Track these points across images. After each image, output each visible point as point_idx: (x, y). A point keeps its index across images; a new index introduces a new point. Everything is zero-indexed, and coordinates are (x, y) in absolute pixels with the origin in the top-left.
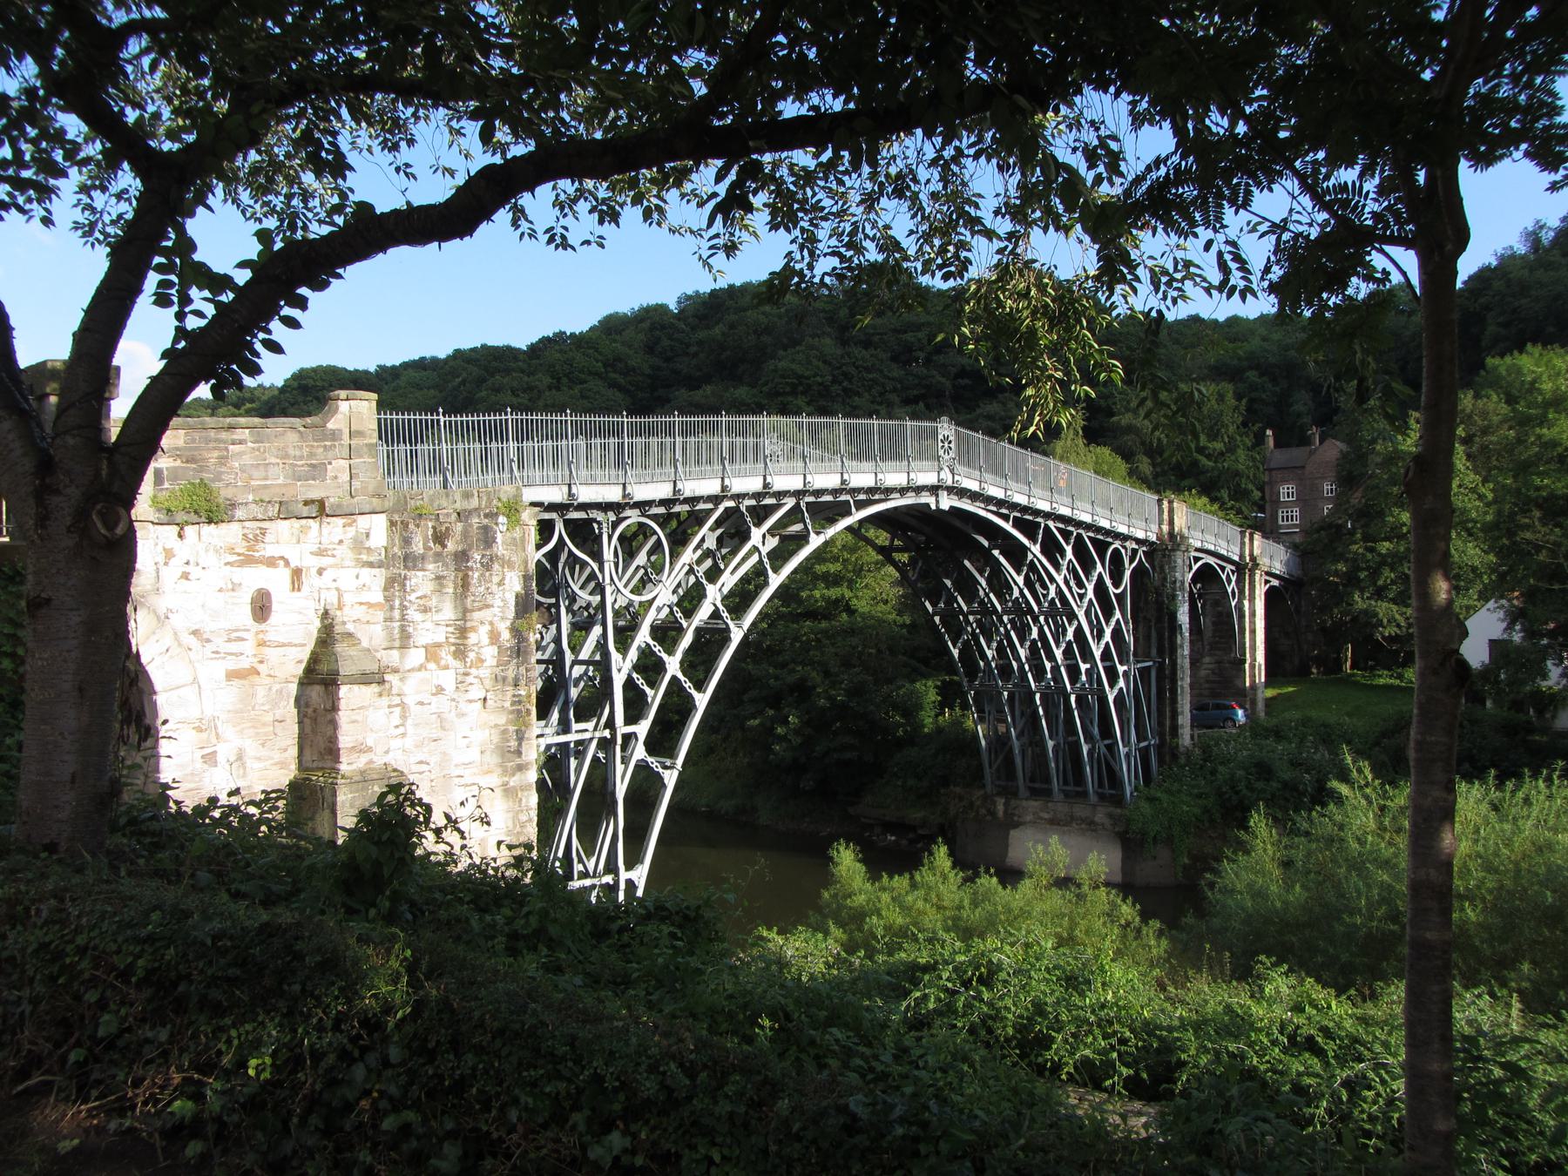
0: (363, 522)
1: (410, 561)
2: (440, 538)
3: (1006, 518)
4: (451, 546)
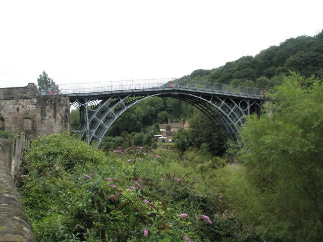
0: (33, 99)
1: (46, 105)
2: (51, 101)
3: (199, 96)
4: (53, 102)
